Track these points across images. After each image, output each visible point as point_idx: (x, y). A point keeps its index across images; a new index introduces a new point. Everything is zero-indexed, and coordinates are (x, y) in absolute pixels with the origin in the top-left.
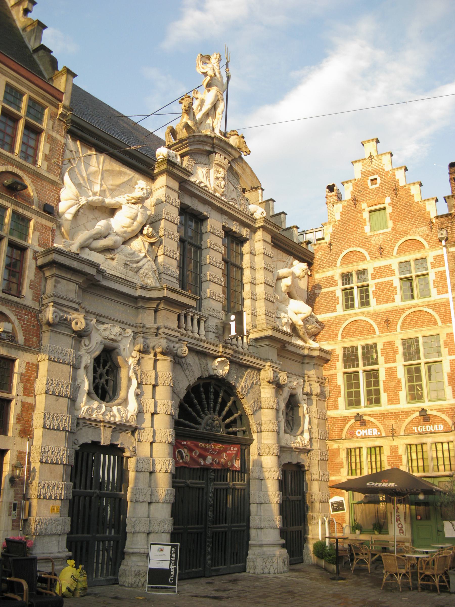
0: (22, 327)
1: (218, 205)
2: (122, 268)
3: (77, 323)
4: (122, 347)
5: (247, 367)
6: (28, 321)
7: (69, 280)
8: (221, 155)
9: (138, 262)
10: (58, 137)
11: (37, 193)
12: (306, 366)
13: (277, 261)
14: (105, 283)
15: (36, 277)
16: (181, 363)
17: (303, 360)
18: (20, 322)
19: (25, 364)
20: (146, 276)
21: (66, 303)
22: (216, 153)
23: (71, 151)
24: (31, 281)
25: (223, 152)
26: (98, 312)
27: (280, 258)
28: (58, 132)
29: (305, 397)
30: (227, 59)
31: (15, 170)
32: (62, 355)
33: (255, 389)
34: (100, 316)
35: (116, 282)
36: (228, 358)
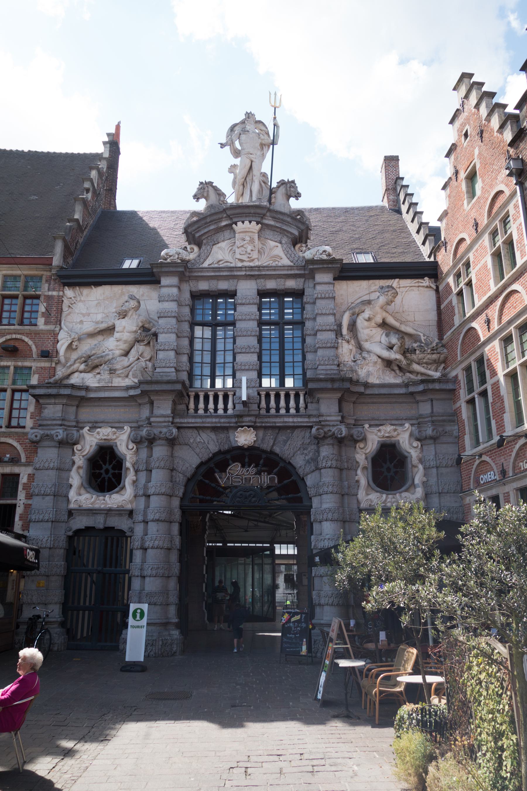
0: (24, 449)
1: (243, 273)
3: (57, 436)
4: (118, 444)
5: (294, 428)
6: (29, 444)
7: (55, 404)
8: (243, 222)
10: (55, 293)
11: (35, 345)
12: (421, 404)
14: (92, 395)
15: (36, 409)
16: (189, 443)
17: (415, 399)
18: (22, 446)
19: (27, 476)
21: (49, 422)
22: (236, 224)
23: (71, 298)
24: (32, 413)
25: (246, 216)
26: (92, 419)
28: (54, 290)
29: (415, 444)
30: (272, 106)
31: (14, 336)
32: (47, 463)
33: (309, 449)
34: (96, 422)
35: (105, 391)
36: (249, 427)
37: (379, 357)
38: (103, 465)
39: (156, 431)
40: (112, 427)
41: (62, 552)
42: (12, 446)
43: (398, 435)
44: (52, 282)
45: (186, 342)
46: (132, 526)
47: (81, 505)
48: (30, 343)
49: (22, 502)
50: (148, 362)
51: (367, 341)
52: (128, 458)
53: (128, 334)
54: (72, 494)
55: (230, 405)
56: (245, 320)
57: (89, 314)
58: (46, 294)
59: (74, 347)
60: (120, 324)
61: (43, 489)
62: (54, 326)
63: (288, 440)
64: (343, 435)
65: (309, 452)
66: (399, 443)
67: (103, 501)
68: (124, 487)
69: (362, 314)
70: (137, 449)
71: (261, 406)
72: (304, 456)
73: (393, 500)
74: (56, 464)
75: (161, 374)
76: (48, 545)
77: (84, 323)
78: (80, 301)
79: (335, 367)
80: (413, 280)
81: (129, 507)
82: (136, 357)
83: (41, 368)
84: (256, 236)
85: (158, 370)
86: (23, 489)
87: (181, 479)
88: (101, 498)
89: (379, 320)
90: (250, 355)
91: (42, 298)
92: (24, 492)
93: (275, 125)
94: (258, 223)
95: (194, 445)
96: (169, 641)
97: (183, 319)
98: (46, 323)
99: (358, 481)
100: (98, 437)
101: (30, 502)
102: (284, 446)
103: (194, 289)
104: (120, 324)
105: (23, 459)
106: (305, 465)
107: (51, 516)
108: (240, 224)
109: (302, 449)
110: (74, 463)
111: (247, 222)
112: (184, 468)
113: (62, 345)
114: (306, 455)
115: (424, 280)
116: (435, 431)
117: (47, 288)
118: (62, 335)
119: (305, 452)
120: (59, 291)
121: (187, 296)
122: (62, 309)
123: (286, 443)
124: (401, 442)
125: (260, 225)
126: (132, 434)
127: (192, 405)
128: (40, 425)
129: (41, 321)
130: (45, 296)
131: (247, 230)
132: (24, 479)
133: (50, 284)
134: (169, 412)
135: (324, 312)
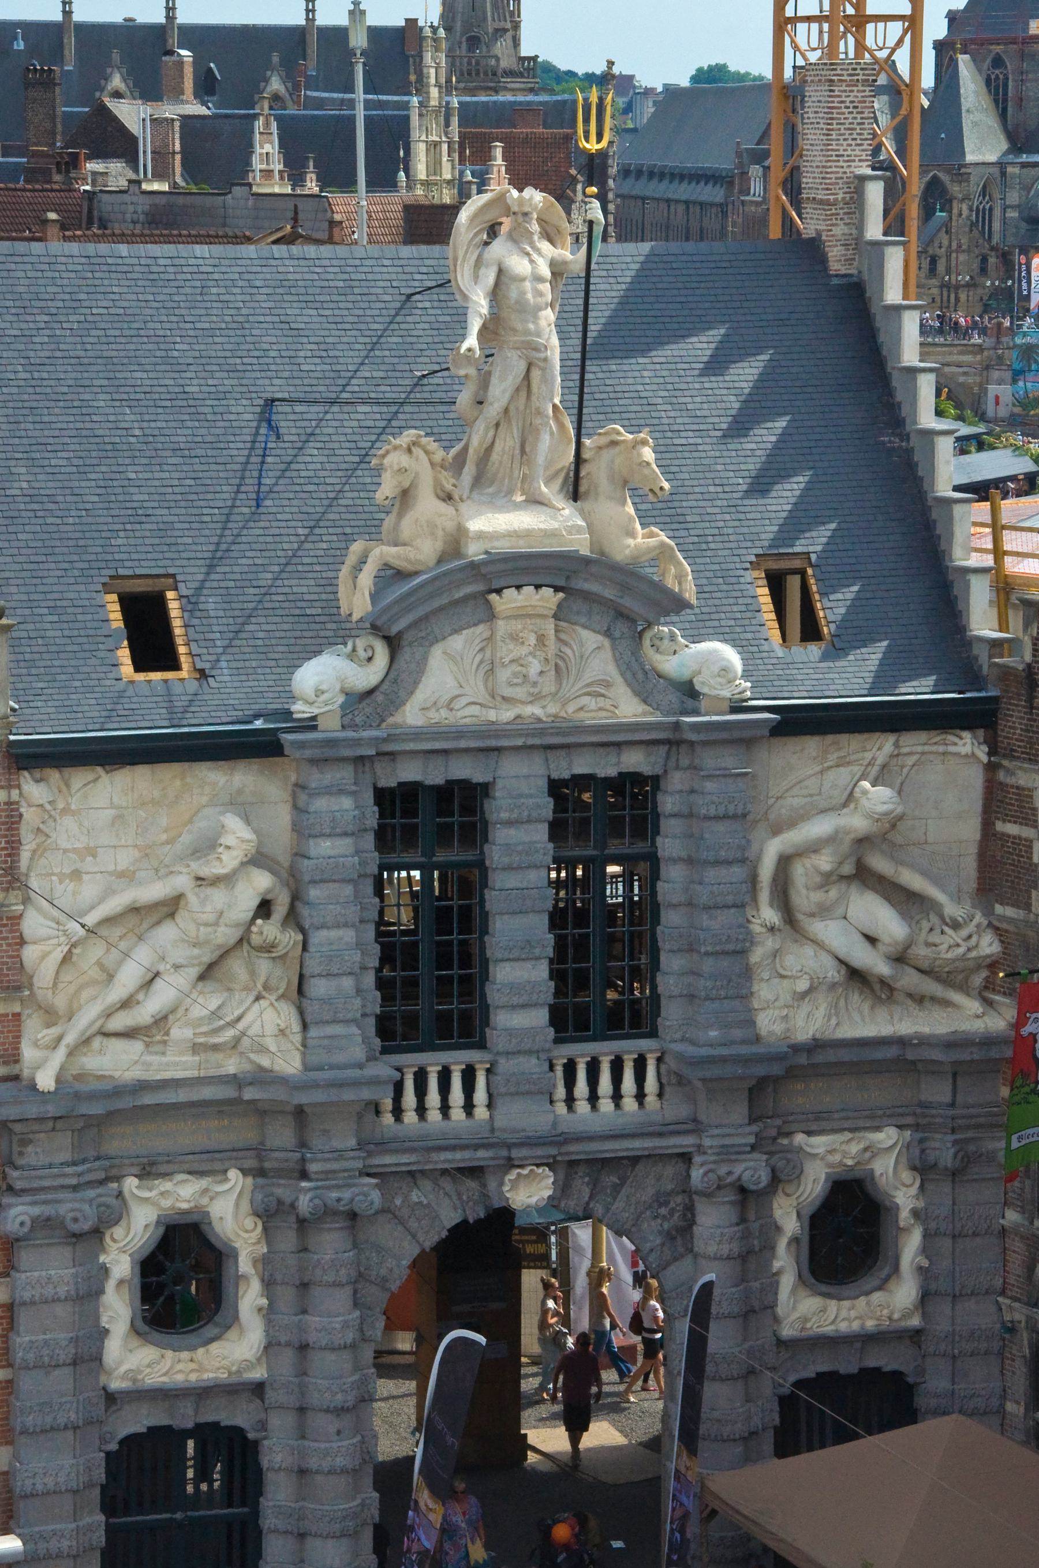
1: (519, 742)
9: (239, 1019)
13: (821, 772)
23: (41, 806)
27: (833, 757)
33: (672, 1205)
36: (538, 1165)
37: (841, 961)
38: (168, 1264)
47: (140, 1377)
51: (812, 915)
53: (228, 931)
55: (480, 1095)
56: (519, 868)
61: (45, 1352)
63: (622, 1185)
64: (762, 1185)
65: (672, 1212)
66: (873, 1178)
69: (813, 856)
72: (659, 1221)
73: (853, 1314)
77: (85, 877)
78: (66, 811)
80: (933, 733)
81: (258, 1374)
82: (255, 993)
84: (549, 626)
90: (529, 965)
94: (557, 589)
95: (405, 1212)
100: (166, 1203)
102: (615, 1198)
103: (382, 783)
106: (663, 1245)
109: (655, 1205)
112: (383, 1272)
115: (961, 738)
119: (663, 1211)
123: (619, 1192)
124: (877, 1173)
125: (561, 595)
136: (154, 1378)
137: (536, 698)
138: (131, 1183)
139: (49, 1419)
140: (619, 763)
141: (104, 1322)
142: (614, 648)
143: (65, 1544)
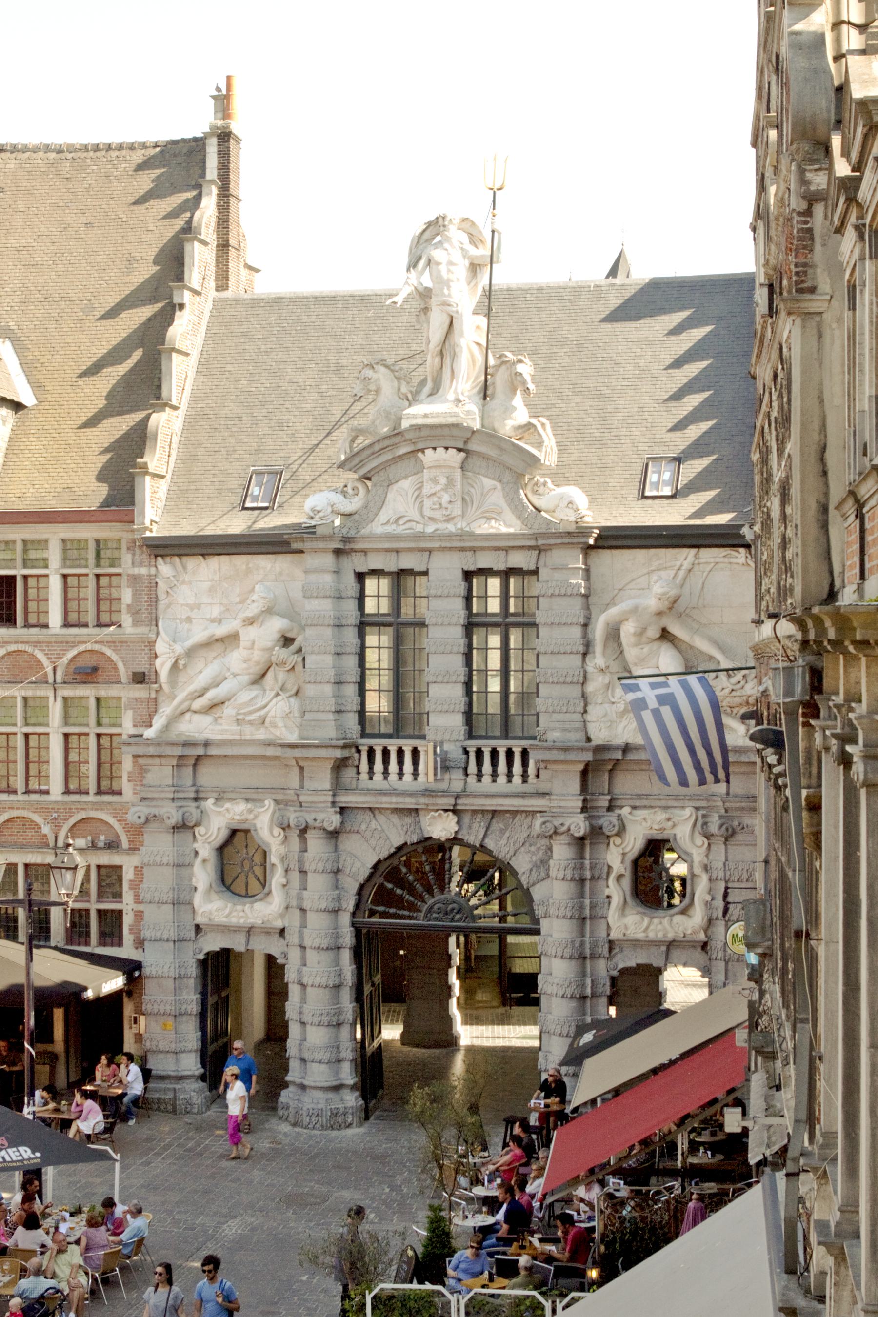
2: (235, 728)
4: (258, 826)
8: (435, 449)
9: (265, 706)
10: (143, 571)
20: (275, 726)
22: (422, 451)
24: (129, 773)
27: (655, 564)
28: (141, 565)
36: (446, 811)
39: (309, 818)
40: (247, 800)
41: (191, 982)
42: (107, 823)
43: (674, 826)
44: (138, 551)
45: (351, 662)
46: (286, 949)
48: (114, 657)
49: (130, 908)
50: (292, 700)
51: (636, 664)
52: (273, 849)
54: (198, 900)
57: (198, 606)
58: (130, 571)
59: (181, 667)
60: (248, 634)
61: (157, 894)
62: (148, 628)
63: (506, 829)
65: (538, 849)
67: (241, 914)
68: (269, 893)
70: (286, 837)
71: (469, 771)
74: (171, 858)
75: (313, 723)
76: (172, 974)
78: (183, 582)
79: (578, 717)
81: (279, 924)
83: (136, 699)
84: (458, 472)
85: (308, 716)
86: (130, 889)
87: (351, 886)
88: (239, 908)
89: (654, 632)
90: (449, 686)
91: (125, 578)
92: (131, 892)
93: (493, 232)
94: (459, 450)
96: (342, 1110)
97: (344, 622)
98: (135, 623)
99: (608, 897)
101: (140, 907)
104: (248, 634)
105: (125, 844)
106: (531, 870)
107: (173, 934)
108: (429, 452)
110: (196, 853)
111: (440, 450)
113: (162, 665)
114: (533, 853)
116: (724, 827)
117: (130, 562)
118: (160, 647)
119: (533, 849)
120: (150, 566)
121: (350, 580)
122: (157, 598)
124: (678, 837)
126: (277, 815)
127: (364, 766)
128: (143, 799)
129: (127, 620)
130: (128, 575)
131: (442, 463)
132: (128, 875)
133: (134, 555)
134: (327, 785)
135: (564, 620)
136: (220, 918)
137: (449, 519)
138: (209, 804)
139: (159, 935)
140: (506, 562)
141: (194, 882)
142: (503, 489)
143: (168, 1008)
